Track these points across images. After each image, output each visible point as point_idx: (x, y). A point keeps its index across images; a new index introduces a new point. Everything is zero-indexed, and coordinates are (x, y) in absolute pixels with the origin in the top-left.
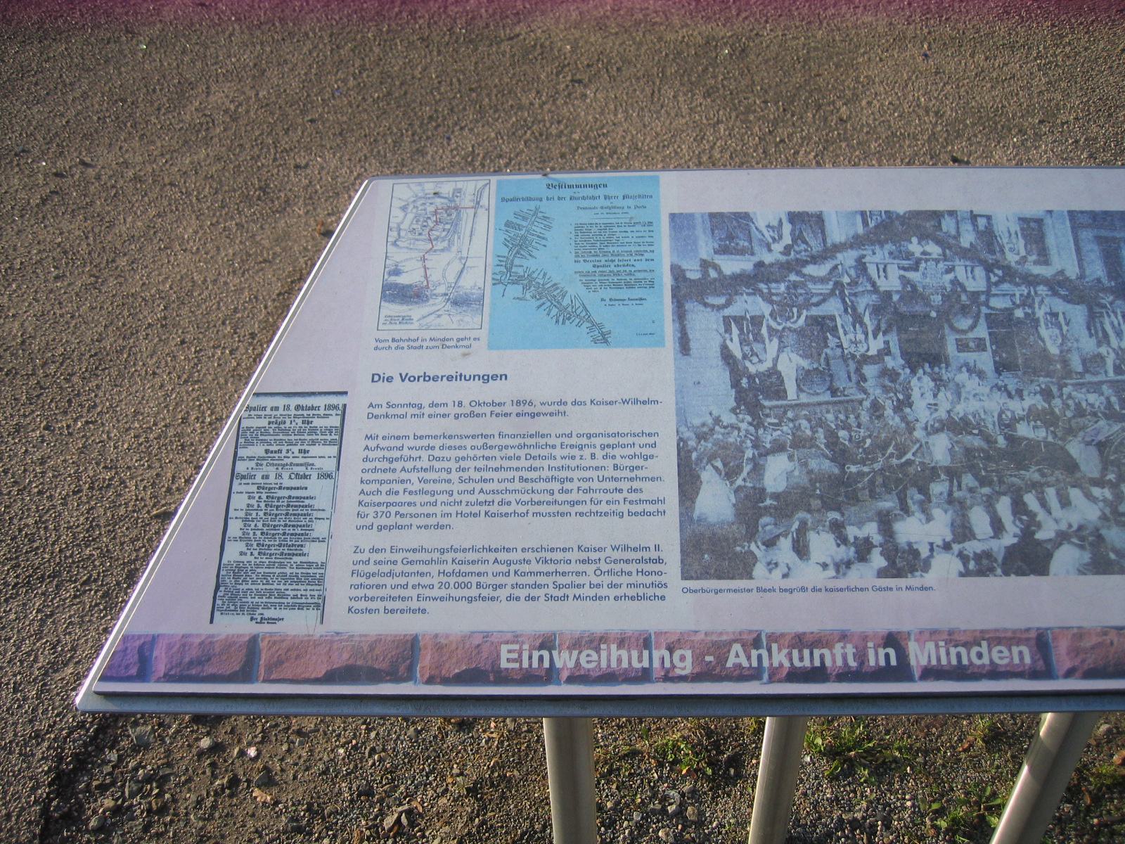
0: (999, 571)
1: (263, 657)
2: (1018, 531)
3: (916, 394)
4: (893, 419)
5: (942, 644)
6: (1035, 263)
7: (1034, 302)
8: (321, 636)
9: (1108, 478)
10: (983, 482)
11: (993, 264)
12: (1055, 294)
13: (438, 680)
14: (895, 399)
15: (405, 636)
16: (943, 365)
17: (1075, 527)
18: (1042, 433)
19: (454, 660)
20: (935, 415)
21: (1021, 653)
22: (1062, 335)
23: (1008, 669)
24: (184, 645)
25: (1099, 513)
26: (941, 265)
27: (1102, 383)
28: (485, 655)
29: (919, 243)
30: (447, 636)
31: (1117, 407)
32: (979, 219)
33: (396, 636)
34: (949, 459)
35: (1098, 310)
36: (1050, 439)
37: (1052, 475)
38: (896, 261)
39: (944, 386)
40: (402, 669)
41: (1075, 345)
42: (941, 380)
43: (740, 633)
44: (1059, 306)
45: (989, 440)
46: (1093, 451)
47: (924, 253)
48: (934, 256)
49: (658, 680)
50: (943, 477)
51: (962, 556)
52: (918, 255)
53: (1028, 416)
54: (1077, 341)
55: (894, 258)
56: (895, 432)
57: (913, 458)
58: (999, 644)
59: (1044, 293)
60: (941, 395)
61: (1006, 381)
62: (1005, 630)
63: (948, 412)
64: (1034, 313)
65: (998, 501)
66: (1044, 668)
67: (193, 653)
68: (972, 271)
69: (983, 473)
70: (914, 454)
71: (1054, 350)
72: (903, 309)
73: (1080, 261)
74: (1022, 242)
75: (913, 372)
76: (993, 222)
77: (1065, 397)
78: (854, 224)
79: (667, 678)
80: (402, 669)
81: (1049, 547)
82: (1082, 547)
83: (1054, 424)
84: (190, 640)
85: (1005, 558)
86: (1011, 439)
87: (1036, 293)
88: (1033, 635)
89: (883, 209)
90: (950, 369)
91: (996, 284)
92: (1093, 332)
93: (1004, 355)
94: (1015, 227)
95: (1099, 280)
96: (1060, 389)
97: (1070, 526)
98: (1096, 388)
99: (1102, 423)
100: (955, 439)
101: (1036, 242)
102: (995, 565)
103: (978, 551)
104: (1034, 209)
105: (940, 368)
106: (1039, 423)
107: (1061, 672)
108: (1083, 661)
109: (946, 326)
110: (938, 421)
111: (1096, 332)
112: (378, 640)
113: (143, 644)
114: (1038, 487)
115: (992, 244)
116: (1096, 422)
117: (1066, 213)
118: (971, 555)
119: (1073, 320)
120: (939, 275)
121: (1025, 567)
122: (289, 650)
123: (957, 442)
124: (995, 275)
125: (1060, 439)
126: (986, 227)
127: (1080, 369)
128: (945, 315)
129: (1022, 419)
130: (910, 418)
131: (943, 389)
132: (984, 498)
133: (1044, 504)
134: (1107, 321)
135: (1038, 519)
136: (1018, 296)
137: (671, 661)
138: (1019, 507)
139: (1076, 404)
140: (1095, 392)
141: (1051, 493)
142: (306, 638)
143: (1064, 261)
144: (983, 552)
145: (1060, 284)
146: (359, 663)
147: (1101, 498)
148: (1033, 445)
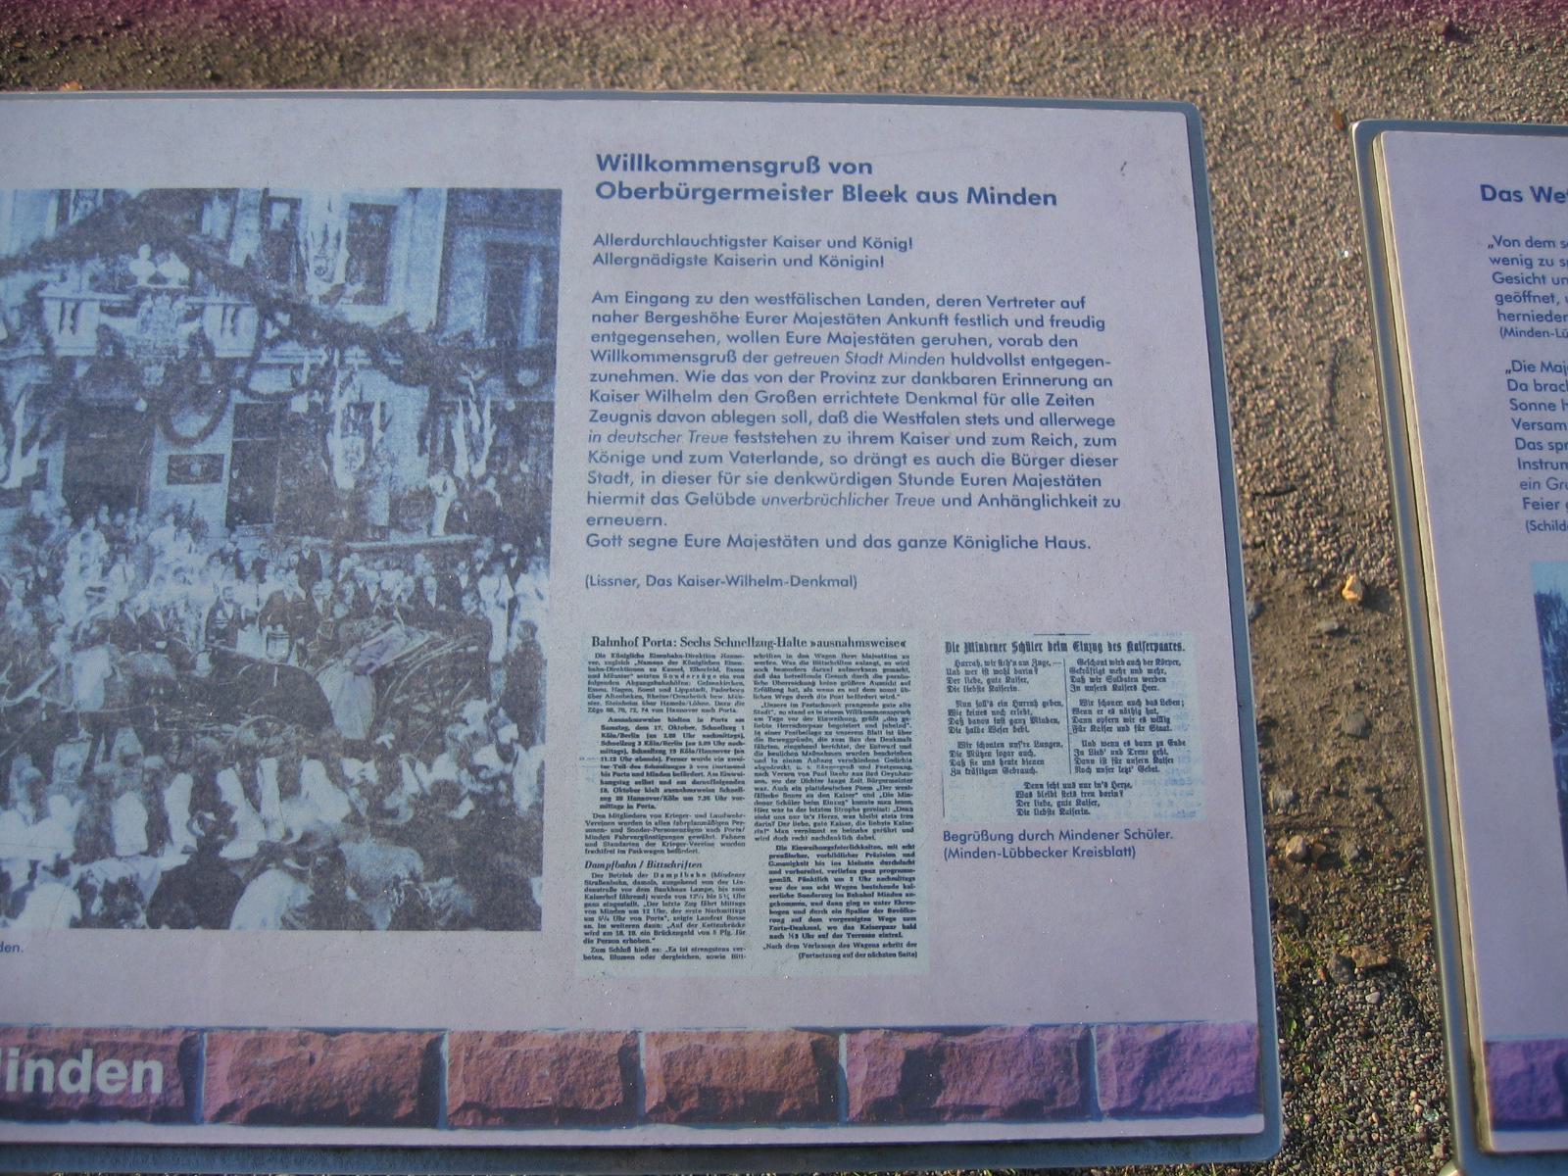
0: (142, 919)
2: (192, 842)
3: (71, 568)
4: (19, 618)
5: (14, 1052)
6: (359, 299)
7: (332, 383)
9: (379, 741)
10: (152, 745)
11: (277, 302)
12: (377, 363)
14: (32, 577)
16: (134, 510)
17: (297, 836)
18: (281, 649)
20: (95, 611)
21: (147, 1073)
22: (369, 450)
23: (120, 1102)
25: (346, 810)
26: (180, 304)
27: (417, 548)
29: (152, 258)
31: (432, 599)
32: (276, 207)
34: (101, 700)
35: (448, 397)
36: (293, 662)
37: (278, 733)
38: (100, 296)
39: (127, 552)
41: (388, 469)
42: (123, 541)
44: (377, 387)
45: (181, 661)
46: (366, 685)
47: (156, 279)
48: (173, 285)
50: (83, 733)
51: (84, 890)
52: (142, 282)
53: (264, 614)
54: (393, 461)
55: (97, 290)
56: (17, 643)
57: (37, 696)
58: (113, 1055)
59: (356, 363)
60: (117, 569)
61: (240, 545)
62: (130, 1030)
63: (121, 605)
64: (327, 404)
65: (169, 782)
66: (181, 1104)
68: (235, 317)
69: (156, 728)
70: (41, 689)
71: (345, 481)
72: (90, 394)
73: (444, 293)
74: (344, 253)
75: (78, 523)
76: (302, 212)
77: (341, 576)
78: (41, 218)
81: (241, 874)
82: (299, 876)
83: (307, 632)
85: (158, 894)
86: (223, 662)
87: (342, 362)
88: (176, 1040)
89: (102, 186)
90: (144, 517)
91: (272, 344)
92: (428, 443)
93: (250, 490)
94: (339, 224)
95: (468, 336)
96: (336, 561)
97: (289, 834)
98: (402, 560)
99: (396, 630)
100: (122, 659)
101: (371, 256)
102: (138, 906)
103: (114, 879)
104: (381, 187)
105: (127, 516)
106: (280, 628)
107: (212, 1111)
109: (158, 430)
110: (99, 622)
111: (434, 446)
114: (246, 757)
115: (287, 258)
116: (385, 630)
117: (444, 195)
118: (100, 887)
119: (397, 420)
120: (172, 325)
121: (190, 913)
123: (123, 665)
124: (276, 324)
125: (312, 662)
126: (285, 225)
127: (383, 519)
128: (163, 406)
129: (251, 620)
130: (51, 616)
131: (122, 558)
132: (147, 777)
133: (251, 791)
134: (459, 422)
135: (233, 820)
136: (306, 369)
138: (205, 796)
139: (357, 592)
140: (399, 567)
141: (269, 767)
143: (412, 298)
144: (123, 881)
145: (392, 344)
147: (358, 780)
148: (259, 672)
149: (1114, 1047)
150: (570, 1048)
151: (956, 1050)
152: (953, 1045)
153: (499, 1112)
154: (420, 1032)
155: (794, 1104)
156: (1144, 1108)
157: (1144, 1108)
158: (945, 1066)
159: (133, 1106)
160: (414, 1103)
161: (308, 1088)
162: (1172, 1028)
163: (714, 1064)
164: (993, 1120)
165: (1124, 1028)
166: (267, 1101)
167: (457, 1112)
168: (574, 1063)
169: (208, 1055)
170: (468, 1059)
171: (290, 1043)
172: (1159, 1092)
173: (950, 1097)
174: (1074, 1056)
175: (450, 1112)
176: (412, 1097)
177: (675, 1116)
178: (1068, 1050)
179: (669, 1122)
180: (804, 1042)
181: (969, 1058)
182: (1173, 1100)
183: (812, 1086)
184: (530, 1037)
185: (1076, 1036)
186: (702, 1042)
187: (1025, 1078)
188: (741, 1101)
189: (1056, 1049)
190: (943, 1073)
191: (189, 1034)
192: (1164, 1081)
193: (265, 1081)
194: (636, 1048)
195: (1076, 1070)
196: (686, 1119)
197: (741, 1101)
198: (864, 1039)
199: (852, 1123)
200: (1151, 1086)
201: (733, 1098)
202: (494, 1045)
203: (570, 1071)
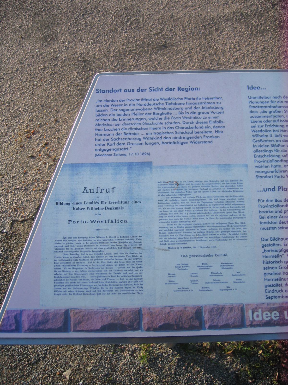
1: (72, 320)
8: (97, 310)
13: (152, 329)
15: (135, 309)
19: (158, 320)
24: (35, 315)
28: (171, 317)
30: (154, 308)
33: (131, 309)
40: (135, 324)
43: (282, 303)
49: (248, 327)
67: (40, 318)
79: (252, 325)
80: (135, 324)
84: (38, 312)
112: (123, 311)
113: (17, 314)
122: (83, 317)
137: (253, 318)
142: (90, 311)
146: (116, 322)
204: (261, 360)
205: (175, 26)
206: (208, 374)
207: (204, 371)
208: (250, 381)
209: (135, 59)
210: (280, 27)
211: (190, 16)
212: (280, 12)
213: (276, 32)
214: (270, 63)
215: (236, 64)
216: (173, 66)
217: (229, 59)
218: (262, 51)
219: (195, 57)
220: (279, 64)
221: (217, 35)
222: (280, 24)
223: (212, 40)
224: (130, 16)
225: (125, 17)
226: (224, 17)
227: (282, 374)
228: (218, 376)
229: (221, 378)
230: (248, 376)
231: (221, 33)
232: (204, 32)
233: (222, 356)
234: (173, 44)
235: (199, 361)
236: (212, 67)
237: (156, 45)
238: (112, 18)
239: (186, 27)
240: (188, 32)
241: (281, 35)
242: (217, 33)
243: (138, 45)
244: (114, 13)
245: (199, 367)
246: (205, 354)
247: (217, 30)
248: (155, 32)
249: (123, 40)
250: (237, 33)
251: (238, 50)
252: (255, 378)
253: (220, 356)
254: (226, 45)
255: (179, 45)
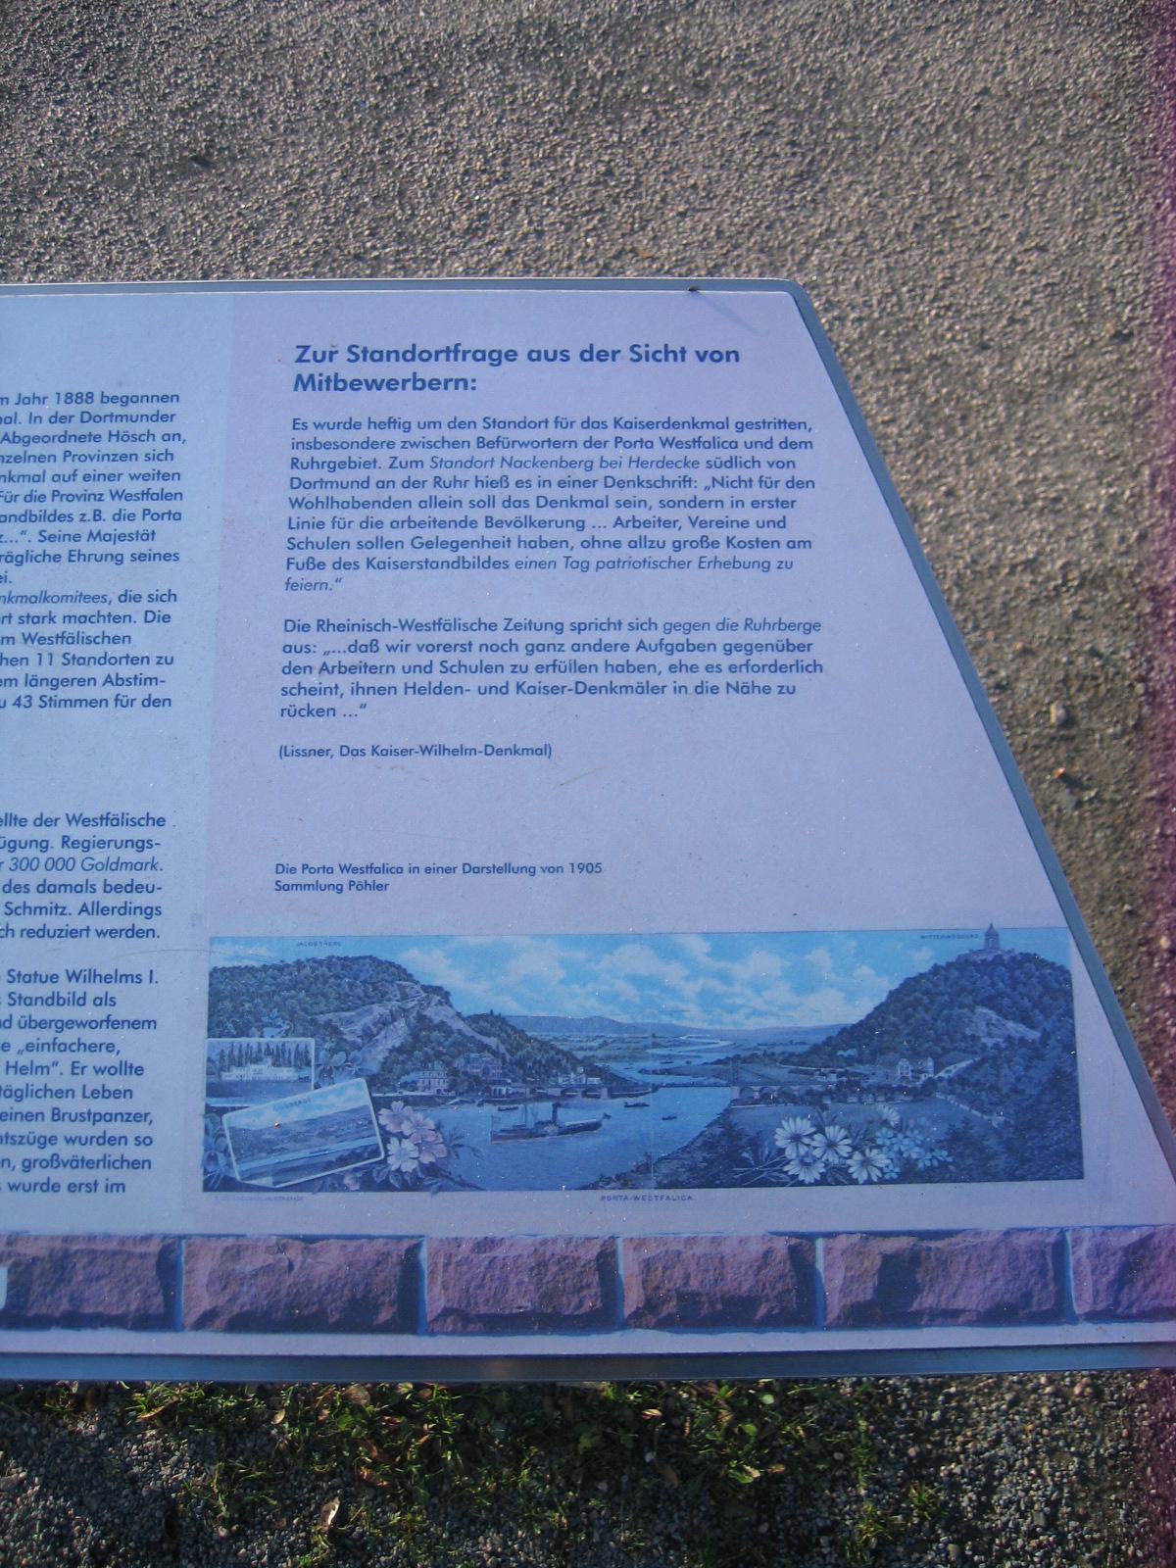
23: (101, 1309)
62: (108, 1237)
88: (154, 1247)
107: (192, 1318)
108: (233, 1299)
149: (1090, 1250)
150: (548, 1254)
151: (932, 1254)
152: (929, 1249)
153: (480, 1317)
154: (399, 1239)
155: (773, 1309)
156: (1119, 1311)
157: (1119, 1311)
158: (922, 1270)
159: (114, 1313)
160: (394, 1310)
161: (288, 1294)
162: (1146, 1231)
163: (693, 1268)
164: (970, 1323)
165: (1098, 1231)
166: (247, 1308)
167: (438, 1316)
168: (554, 1269)
169: (187, 1262)
170: (447, 1265)
171: (268, 1249)
172: (1134, 1295)
173: (927, 1301)
174: (1049, 1259)
175: (429, 1319)
176: (392, 1304)
177: (654, 1321)
178: (1043, 1253)
179: (648, 1327)
180: (781, 1246)
181: (944, 1263)
182: (1147, 1304)
183: (789, 1291)
184: (507, 1243)
185: (1052, 1239)
186: (680, 1247)
187: (1000, 1283)
188: (719, 1307)
189: (1030, 1252)
190: (919, 1277)
191: (166, 1243)
192: (1140, 1284)
193: (245, 1289)
194: (614, 1253)
195: (1051, 1274)
196: (666, 1324)
197: (719, 1307)
198: (842, 1243)
199: (830, 1327)
200: (1126, 1290)
201: (712, 1303)
202: (472, 1251)
203: (549, 1277)
204: (279, 1452)
205: (264, 76)
206: (57, 1498)
207: (44, 1485)
208: (223, 1532)
209: (69, 212)
210: (696, 85)
211: (337, 37)
212: (713, 27)
213: (678, 107)
214: (619, 233)
215: (475, 234)
216: (215, 242)
217: (453, 216)
218: (598, 183)
219: (313, 208)
220: (655, 238)
221: (429, 115)
222: (701, 73)
223: (399, 137)
224: (95, 33)
225: (75, 37)
226: (473, 42)
227: (358, 1508)
228: (94, 1506)
229: (107, 1515)
230: (217, 1511)
231: (444, 109)
232: (377, 105)
233: (123, 1428)
234: (241, 151)
235: (30, 1442)
236: (374, 247)
237: (172, 154)
238: (21, 40)
239: (309, 81)
240: (313, 103)
241: (691, 120)
242: (430, 107)
243: (95, 157)
244: (35, 20)
245: (24, 1465)
246: (59, 1416)
247: (432, 95)
248: (178, 101)
249: (41, 134)
250: (513, 111)
251: (498, 181)
252: (246, 1521)
253: (121, 1423)
254: (453, 159)
255: (265, 155)
